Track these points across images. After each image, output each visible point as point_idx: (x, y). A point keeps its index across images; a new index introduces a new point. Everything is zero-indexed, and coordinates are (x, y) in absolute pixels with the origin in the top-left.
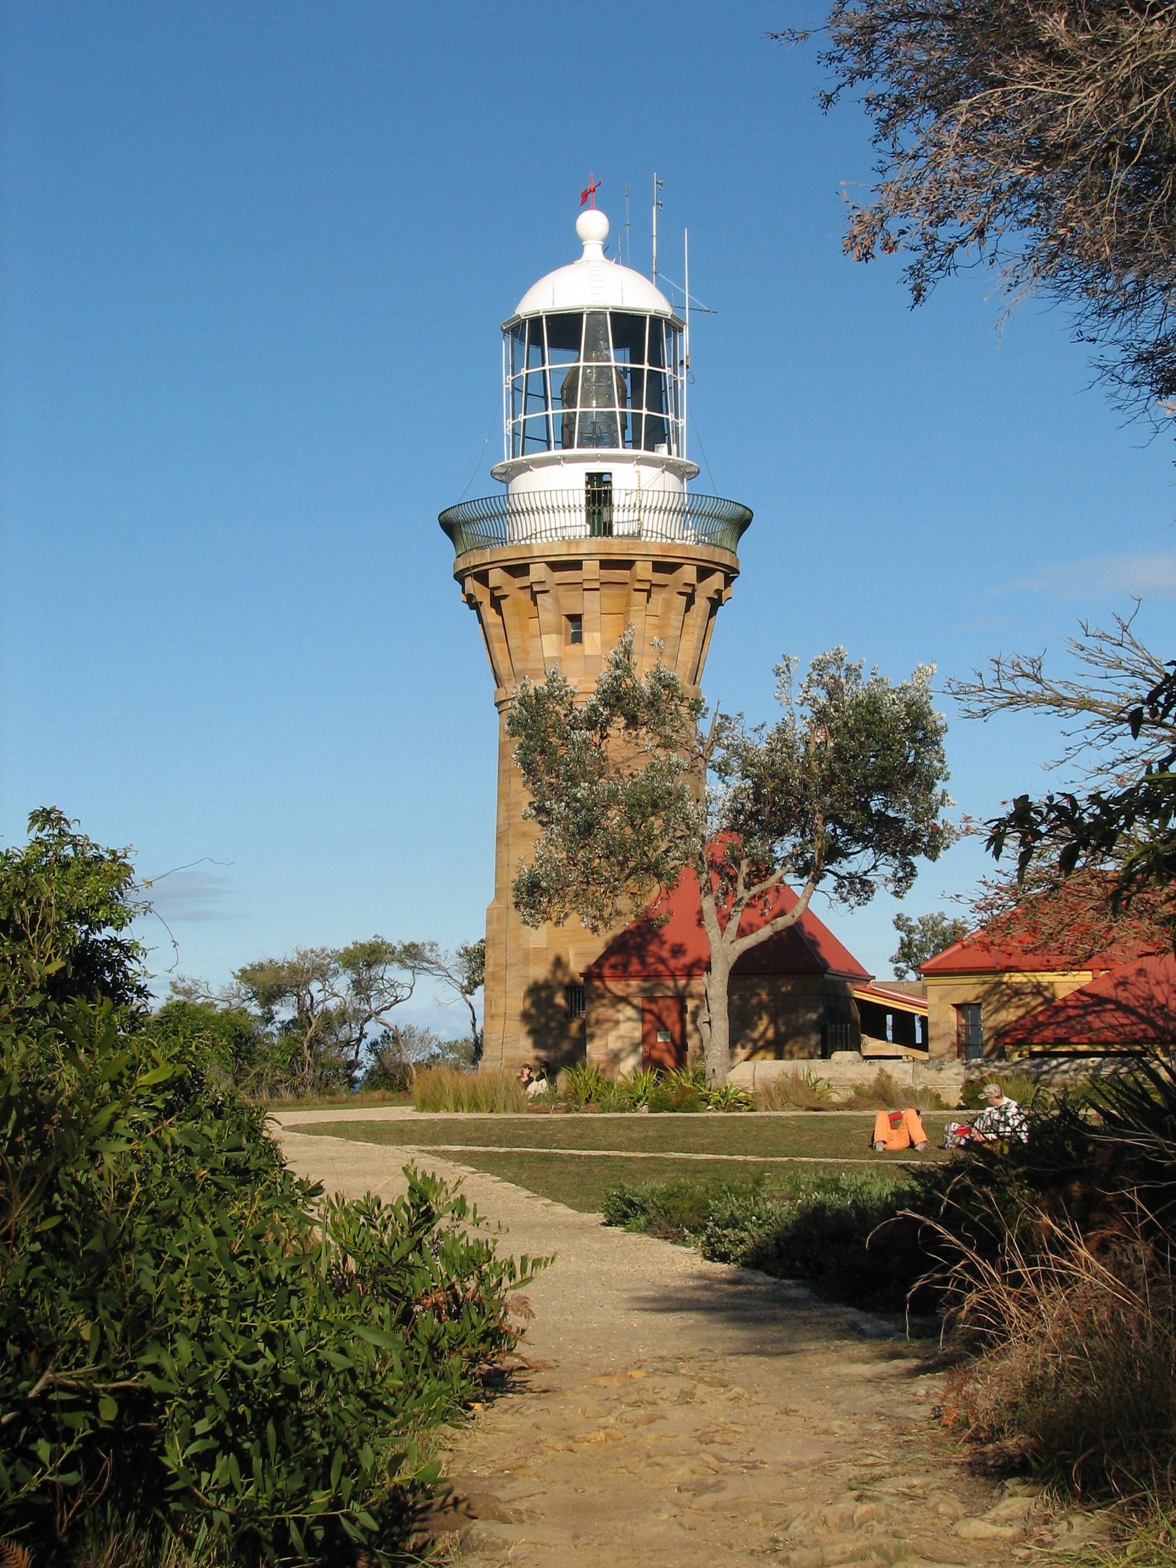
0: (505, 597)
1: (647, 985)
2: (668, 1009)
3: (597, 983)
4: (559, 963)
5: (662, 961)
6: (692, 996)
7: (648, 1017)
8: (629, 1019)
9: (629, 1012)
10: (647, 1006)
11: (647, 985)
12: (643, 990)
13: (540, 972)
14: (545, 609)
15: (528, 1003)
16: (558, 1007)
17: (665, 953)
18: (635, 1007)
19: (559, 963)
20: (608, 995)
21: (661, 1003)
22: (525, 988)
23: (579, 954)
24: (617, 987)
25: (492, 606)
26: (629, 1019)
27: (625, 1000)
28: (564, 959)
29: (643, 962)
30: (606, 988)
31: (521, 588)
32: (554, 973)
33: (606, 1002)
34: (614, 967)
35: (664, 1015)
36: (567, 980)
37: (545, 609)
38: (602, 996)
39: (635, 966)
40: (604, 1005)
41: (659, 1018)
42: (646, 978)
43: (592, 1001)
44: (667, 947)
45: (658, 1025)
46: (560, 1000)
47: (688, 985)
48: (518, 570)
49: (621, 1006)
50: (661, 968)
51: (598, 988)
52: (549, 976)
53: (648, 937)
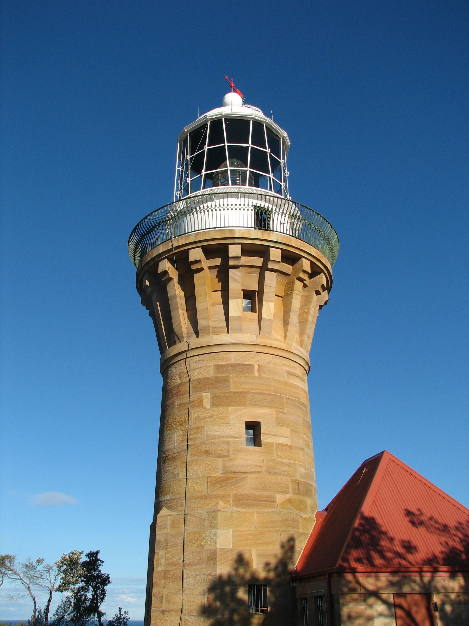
0: (202, 269)
1: (395, 579)
2: (416, 604)
3: (349, 577)
4: (241, 560)
5: (398, 555)
6: (438, 592)
7: (399, 612)
8: (381, 615)
9: (380, 608)
10: (398, 601)
11: (395, 579)
12: (392, 584)
13: (224, 569)
14: (235, 280)
15: (212, 596)
16: (240, 602)
17: (400, 550)
18: (385, 602)
19: (241, 560)
20: (361, 590)
21: (409, 598)
22: (205, 586)
23: (259, 556)
24: (369, 583)
25: (179, 283)
26: (381, 615)
27: (375, 594)
28: (246, 556)
29: (383, 557)
30: (358, 582)
31: (210, 268)
32: (236, 569)
33: (355, 596)
34: (358, 560)
35: (414, 610)
36: (248, 576)
37: (235, 280)
38: (353, 590)
39: (378, 561)
40: (356, 600)
41: (408, 614)
42: (393, 573)
43: (344, 594)
44: (396, 542)
45: (408, 621)
46: (242, 594)
47: (433, 578)
48: (216, 249)
49: (371, 600)
50: (404, 562)
51: (350, 582)
52: (233, 572)
53: (374, 533)
